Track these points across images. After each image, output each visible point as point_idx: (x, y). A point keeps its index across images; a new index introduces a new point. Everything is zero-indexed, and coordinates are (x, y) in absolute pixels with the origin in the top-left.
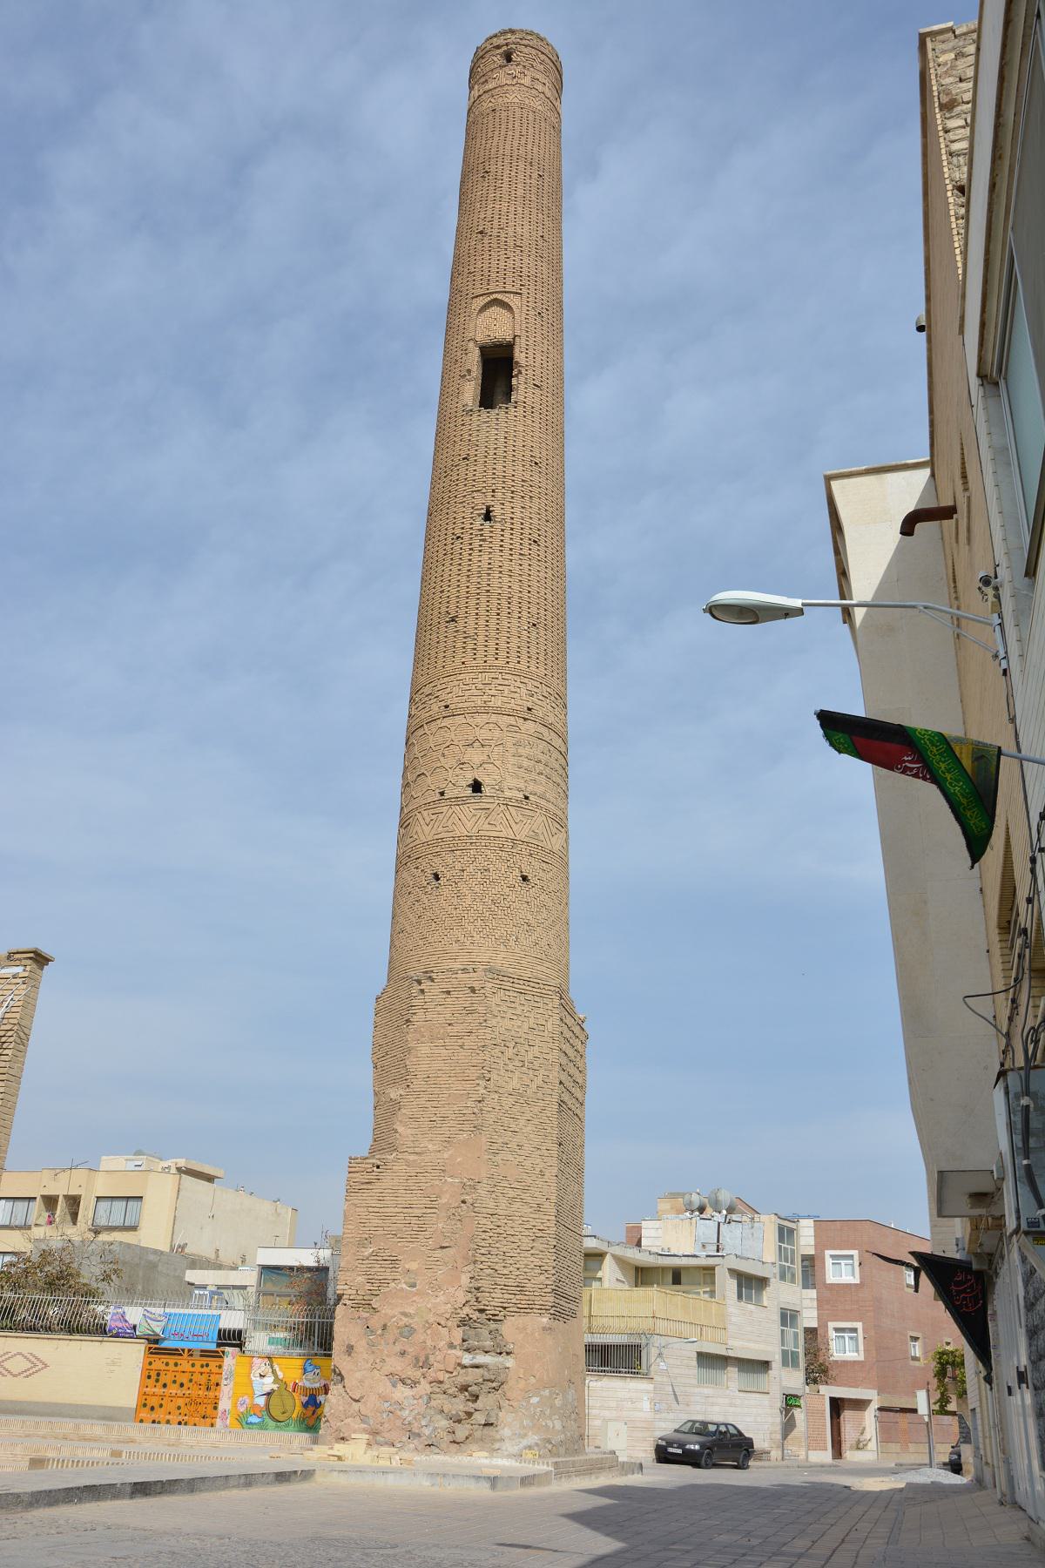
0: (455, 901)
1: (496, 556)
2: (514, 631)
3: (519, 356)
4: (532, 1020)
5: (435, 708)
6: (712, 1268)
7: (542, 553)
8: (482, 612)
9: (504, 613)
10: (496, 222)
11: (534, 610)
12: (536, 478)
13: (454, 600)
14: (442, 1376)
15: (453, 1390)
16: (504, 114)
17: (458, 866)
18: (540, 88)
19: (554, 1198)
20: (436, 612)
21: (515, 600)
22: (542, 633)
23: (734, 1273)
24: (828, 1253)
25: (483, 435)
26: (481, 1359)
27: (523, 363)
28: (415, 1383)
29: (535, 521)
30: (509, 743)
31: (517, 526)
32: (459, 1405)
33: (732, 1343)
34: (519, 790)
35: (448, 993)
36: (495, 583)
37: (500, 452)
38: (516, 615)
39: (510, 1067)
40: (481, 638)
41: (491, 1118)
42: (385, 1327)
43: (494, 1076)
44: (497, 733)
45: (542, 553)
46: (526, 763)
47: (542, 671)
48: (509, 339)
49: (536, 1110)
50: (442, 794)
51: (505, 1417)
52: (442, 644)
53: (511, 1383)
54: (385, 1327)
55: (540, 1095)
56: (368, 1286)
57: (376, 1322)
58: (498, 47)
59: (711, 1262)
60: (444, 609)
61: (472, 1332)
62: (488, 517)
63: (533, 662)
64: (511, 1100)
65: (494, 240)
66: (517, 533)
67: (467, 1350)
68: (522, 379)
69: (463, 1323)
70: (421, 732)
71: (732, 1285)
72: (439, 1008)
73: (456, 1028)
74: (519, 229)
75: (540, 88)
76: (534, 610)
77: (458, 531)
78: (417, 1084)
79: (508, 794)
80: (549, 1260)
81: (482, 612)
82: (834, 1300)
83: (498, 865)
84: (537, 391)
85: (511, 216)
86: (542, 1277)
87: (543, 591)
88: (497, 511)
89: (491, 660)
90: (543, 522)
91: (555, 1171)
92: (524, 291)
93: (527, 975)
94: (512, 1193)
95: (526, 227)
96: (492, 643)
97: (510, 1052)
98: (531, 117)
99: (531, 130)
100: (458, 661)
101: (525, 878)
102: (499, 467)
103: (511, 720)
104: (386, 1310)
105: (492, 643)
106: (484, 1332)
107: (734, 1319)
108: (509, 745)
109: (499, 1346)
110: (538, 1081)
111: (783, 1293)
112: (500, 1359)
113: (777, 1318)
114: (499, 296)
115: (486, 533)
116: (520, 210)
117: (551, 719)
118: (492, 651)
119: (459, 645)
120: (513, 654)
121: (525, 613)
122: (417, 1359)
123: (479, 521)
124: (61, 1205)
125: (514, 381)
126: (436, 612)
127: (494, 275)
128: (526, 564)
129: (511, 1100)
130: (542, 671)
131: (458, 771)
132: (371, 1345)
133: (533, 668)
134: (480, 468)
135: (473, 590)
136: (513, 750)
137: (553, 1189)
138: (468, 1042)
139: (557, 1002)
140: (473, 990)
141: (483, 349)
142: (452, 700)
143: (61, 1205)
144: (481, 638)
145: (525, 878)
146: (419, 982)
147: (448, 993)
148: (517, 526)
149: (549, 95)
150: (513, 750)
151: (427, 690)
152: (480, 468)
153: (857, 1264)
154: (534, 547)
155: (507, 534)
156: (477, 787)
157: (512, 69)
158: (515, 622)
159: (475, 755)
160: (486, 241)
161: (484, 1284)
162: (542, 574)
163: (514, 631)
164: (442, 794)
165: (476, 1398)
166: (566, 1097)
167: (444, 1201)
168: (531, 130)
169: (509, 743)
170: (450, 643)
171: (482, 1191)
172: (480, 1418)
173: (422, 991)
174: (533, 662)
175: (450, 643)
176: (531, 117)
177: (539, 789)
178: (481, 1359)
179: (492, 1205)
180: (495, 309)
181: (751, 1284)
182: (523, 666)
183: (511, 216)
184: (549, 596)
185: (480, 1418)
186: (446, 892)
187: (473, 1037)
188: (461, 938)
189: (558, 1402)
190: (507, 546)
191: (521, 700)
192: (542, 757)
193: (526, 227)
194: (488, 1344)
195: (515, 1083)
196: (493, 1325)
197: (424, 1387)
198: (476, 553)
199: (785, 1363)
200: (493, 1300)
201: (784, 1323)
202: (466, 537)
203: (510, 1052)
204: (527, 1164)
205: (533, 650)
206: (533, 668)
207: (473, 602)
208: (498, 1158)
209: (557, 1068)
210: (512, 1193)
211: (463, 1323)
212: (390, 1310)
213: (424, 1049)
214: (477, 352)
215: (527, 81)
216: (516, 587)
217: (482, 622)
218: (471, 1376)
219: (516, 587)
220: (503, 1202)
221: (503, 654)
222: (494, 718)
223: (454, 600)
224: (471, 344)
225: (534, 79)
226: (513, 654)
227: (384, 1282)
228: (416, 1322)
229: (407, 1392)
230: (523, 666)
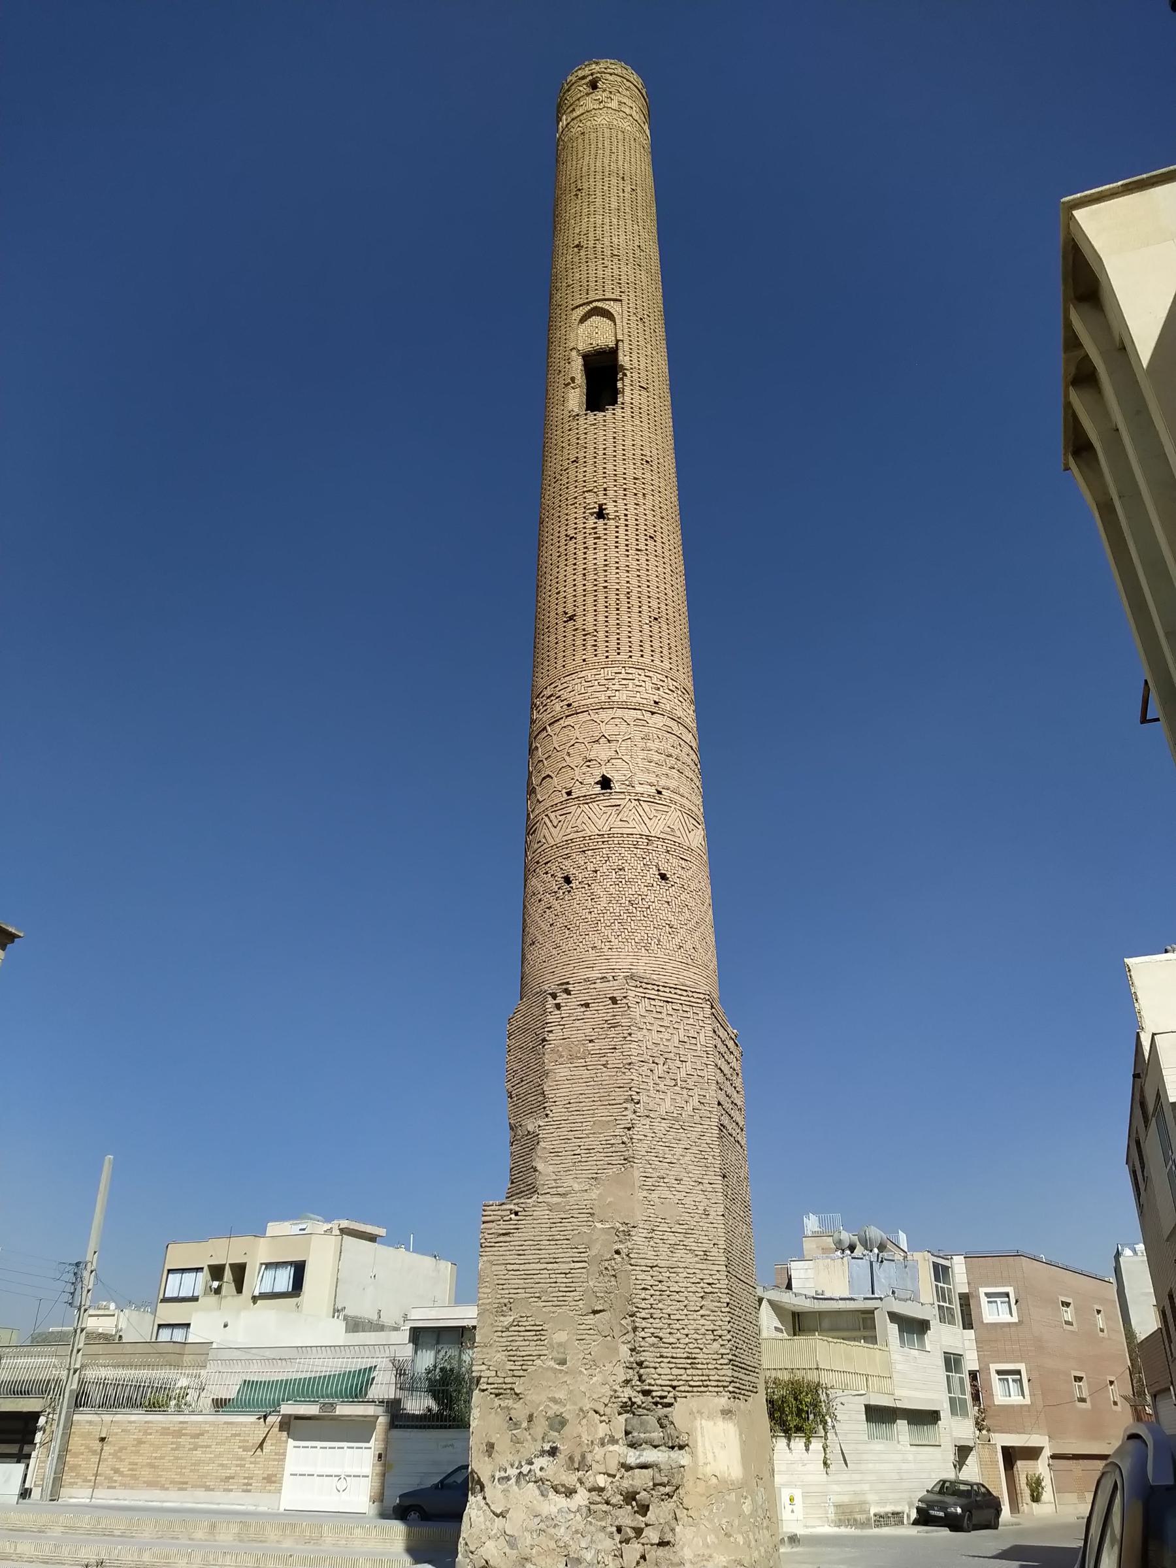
0: (589, 904)
1: (612, 552)
2: (635, 626)
3: (623, 359)
4: (681, 1032)
5: (558, 708)
6: (872, 1312)
7: (660, 551)
8: (601, 607)
9: (624, 608)
10: (591, 235)
11: (654, 604)
12: (648, 475)
13: (570, 600)
14: (602, 1481)
15: (617, 1499)
16: (593, 135)
17: (591, 867)
18: (628, 111)
19: (722, 1244)
20: (553, 614)
21: (634, 595)
22: (665, 627)
23: (894, 1317)
24: (983, 1291)
25: (590, 436)
26: (650, 1455)
27: (627, 366)
28: (570, 1493)
29: (650, 517)
30: (638, 737)
31: (632, 522)
32: (627, 1517)
33: (898, 1393)
34: (651, 785)
35: (587, 1005)
36: (612, 578)
37: (610, 452)
39: (662, 1087)
40: (601, 635)
41: (642, 1148)
42: (530, 1418)
43: (643, 1098)
44: (624, 726)
45: (660, 551)
46: (656, 757)
47: (668, 666)
48: (612, 345)
49: (694, 1135)
50: (569, 794)
51: (684, 1533)
52: (561, 645)
53: (689, 1484)
54: (530, 1418)
55: (697, 1119)
56: (510, 1365)
57: (520, 1411)
58: (584, 78)
59: (870, 1305)
60: (560, 610)
61: (635, 1421)
62: (601, 514)
63: (657, 655)
64: (664, 1124)
65: (591, 251)
66: (632, 529)
67: (632, 1445)
68: (627, 381)
69: (628, 1407)
70: (544, 734)
71: (893, 1329)
72: (577, 1023)
73: (597, 1045)
74: (615, 240)
75: (628, 111)
76: (654, 604)
77: (571, 532)
78: (557, 1112)
79: (639, 789)
80: (722, 1322)
81: (601, 607)
82: (993, 1339)
83: (634, 863)
84: (643, 393)
85: (607, 227)
86: (716, 1345)
87: (662, 587)
88: (610, 509)
89: (613, 656)
90: (658, 518)
91: (721, 1210)
92: (624, 297)
93: (672, 982)
94: (673, 1239)
95: (623, 237)
96: (613, 638)
97: (660, 1070)
98: (620, 136)
99: (621, 148)
101: (663, 877)
102: (610, 466)
103: (638, 714)
104: (531, 1396)
105: (613, 638)
106: (651, 1420)
107: (899, 1367)
108: (638, 739)
109: (670, 1436)
111: (947, 1336)
112: (675, 1454)
113: (942, 1363)
114: (599, 304)
115: (600, 531)
116: (615, 221)
117: (680, 713)
118: (613, 645)
119: (579, 642)
120: (636, 648)
121: (645, 608)
122: (571, 1459)
123: (592, 520)
124: (228, 1275)
125: (619, 385)
126: (553, 614)
127: (592, 284)
128: (643, 558)
130: (666, 662)
131: (585, 769)
132: (516, 1441)
133: (657, 662)
134: (590, 469)
135: (590, 587)
136: (641, 744)
137: (721, 1232)
138: (613, 1059)
139: (708, 1011)
140: (614, 1000)
141: (586, 357)
142: (577, 700)
143: (228, 1275)
144: (601, 635)
145: (663, 877)
146: (554, 996)
147: (587, 1005)
148: (632, 522)
149: (637, 118)
150: (641, 744)
151: (548, 692)
152: (590, 469)
153: (1013, 1301)
154: (650, 542)
155: (622, 530)
156: (605, 783)
157: (599, 95)
158: (635, 616)
159: (602, 752)
160: (583, 253)
161: (646, 1356)
163: (635, 626)
164: (569, 794)
165: (644, 1509)
166: (726, 1120)
167: (594, 1252)
168: (621, 148)
169: (638, 737)
170: (569, 642)
171: (638, 1237)
172: (652, 1535)
173: (558, 1006)
174: (657, 655)
175: (569, 642)
176: (620, 136)
177: (673, 784)
178: (650, 1455)
180: (595, 319)
181: (914, 1328)
182: (647, 659)
183: (607, 227)
184: (669, 591)
185: (652, 1535)
186: (578, 895)
187: (617, 1054)
188: (598, 944)
189: (747, 1508)
190: (622, 542)
191: (647, 694)
192: (671, 751)
193: (623, 237)
194: (657, 1435)
195: (667, 1105)
196: (661, 1411)
197: (582, 1497)
198: (591, 551)
199: (953, 1412)
200: (660, 1376)
201: (948, 1368)
202: (580, 537)
203: (660, 1070)
205: (656, 644)
206: (657, 662)
207: (590, 599)
208: (655, 1195)
209: (714, 1086)
211: (628, 1407)
212: (540, 1396)
213: (562, 1072)
214: (580, 361)
215: (614, 105)
216: (634, 582)
217: (601, 618)
218: (641, 1479)
219: (634, 582)
220: (663, 1249)
221: (624, 648)
222: (620, 713)
223: (570, 600)
224: (574, 353)
225: (620, 103)
226: (636, 648)
227: (527, 1359)
228: (568, 1411)
229: (561, 1501)
230: (647, 659)
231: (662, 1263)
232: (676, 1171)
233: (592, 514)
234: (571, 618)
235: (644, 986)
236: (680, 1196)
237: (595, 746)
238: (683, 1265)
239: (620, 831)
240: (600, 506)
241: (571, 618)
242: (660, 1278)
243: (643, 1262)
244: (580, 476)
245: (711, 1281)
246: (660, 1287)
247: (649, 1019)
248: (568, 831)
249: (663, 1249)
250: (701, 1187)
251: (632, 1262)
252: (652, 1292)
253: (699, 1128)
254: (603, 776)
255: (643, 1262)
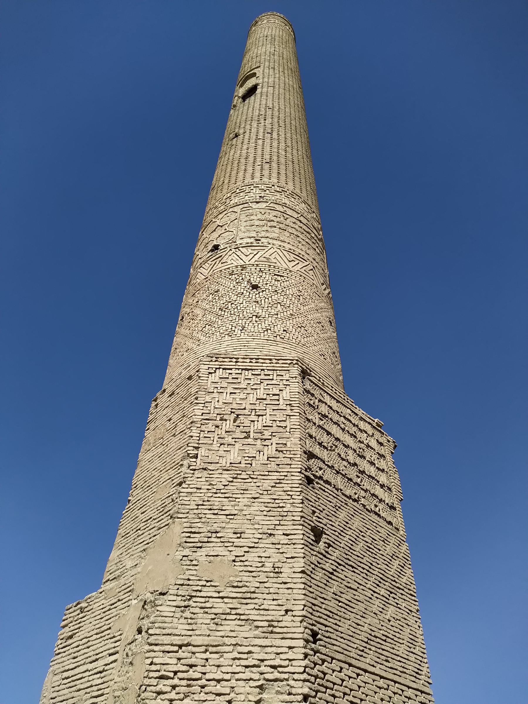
19: (298, 609)
49: (267, 485)
55: (273, 466)
64: (227, 476)
94: (221, 607)
97: (228, 425)
110: (271, 451)
129: (227, 476)
137: (298, 593)
145: (255, 287)
179: (182, 627)
195: (234, 456)
204: (252, 557)
210: (221, 607)
231: (198, 640)
232: (234, 525)
235: (221, 360)
236: (239, 552)
238: (233, 641)
242: (192, 661)
243: (167, 640)
245: (277, 662)
246: (192, 674)
247: (224, 385)
249: (203, 619)
250: (272, 539)
251: (152, 640)
252: (176, 681)
253: (275, 476)
255: (167, 640)
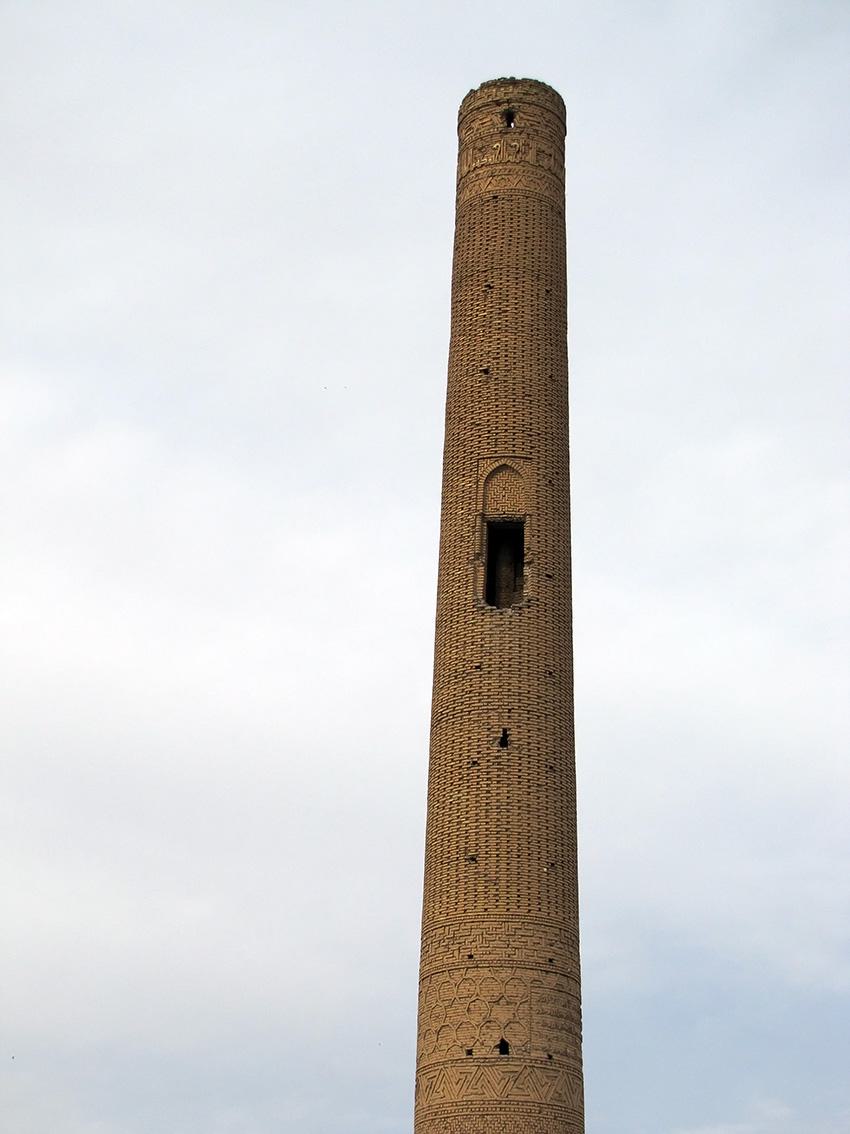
38: (535, 856)
50: (470, 1052)
58: (498, 103)
77: (475, 755)
79: (534, 1055)
88: (513, 736)
100: (480, 908)
121: (544, 853)
131: (484, 1030)
156: (504, 1047)
162: (559, 804)
164: (470, 1052)
198: (494, 785)
202: (484, 764)
207: (493, 841)
219: (535, 824)
233: (495, 738)
234: (473, 859)
237: (496, 1007)
239: (517, 1098)
240: (505, 730)
241: (473, 859)
244: (485, 689)
248: (470, 1091)
254: (503, 1041)
